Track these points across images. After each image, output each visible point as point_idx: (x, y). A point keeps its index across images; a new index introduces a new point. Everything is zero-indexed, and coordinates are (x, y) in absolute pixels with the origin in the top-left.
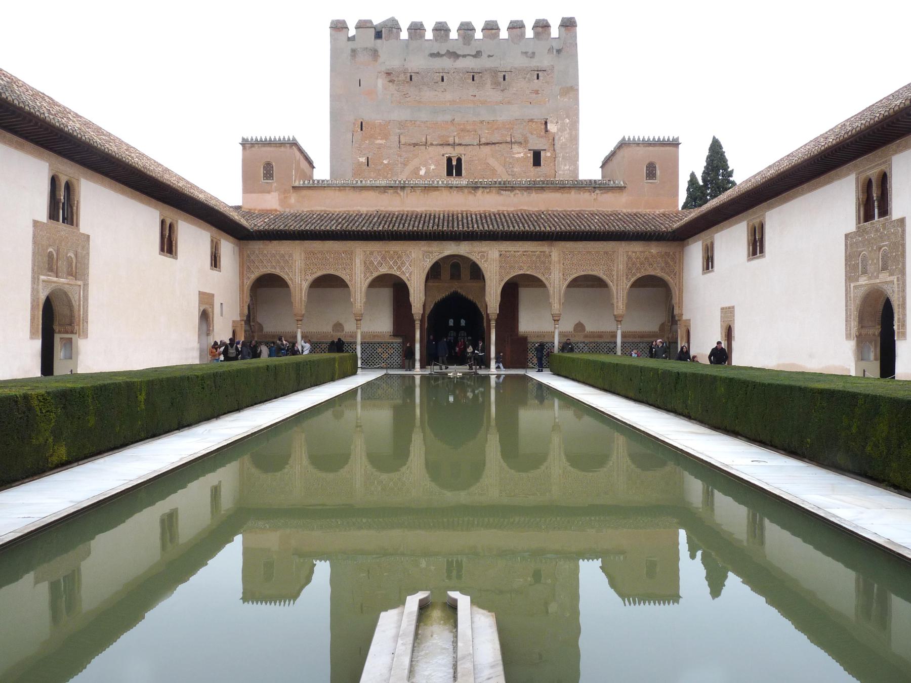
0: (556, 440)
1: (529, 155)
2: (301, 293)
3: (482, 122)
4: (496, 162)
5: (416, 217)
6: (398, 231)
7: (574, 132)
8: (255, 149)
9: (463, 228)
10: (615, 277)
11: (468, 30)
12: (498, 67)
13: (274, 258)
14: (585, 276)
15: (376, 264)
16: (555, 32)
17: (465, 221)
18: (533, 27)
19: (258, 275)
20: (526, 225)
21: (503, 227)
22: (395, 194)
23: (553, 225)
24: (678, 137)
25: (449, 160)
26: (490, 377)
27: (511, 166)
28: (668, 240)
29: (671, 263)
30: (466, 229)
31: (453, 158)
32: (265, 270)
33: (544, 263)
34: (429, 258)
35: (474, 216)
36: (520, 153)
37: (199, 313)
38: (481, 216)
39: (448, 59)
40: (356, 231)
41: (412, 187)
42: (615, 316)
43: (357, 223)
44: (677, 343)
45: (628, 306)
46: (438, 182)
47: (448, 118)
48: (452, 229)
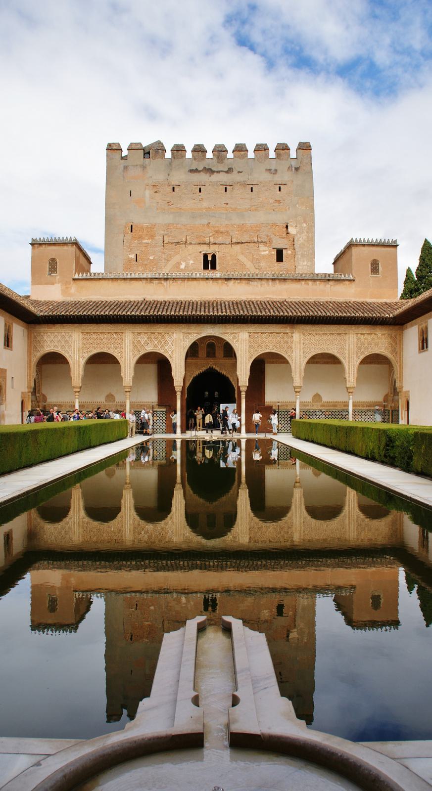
0: (298, 494)
1: (273, 253)
3: (233, 225)
4: (245, 258)
5: (177, 303)
7: (310, 234)
9: (218, 313)
10: (347, 355)
11: (222, 151)
12: (245, 181)
13: (56, 339)
14: (322, 354)
15: (143, 343)
16: (293, 154)
17: (219, 307)
18: (275, 150)
19: (43, 353)
20: (271, 311)
21: (252, 312)
23: (295, 310)
24: (396, 240)
25: (205, 256)
26: (241, 441)
27: (258, 262)
30: (220, 313)
31: (208, 255)
32: (49, 349)
34: (189, 339)
35: (227, 303)
36: (265, 251)
38: (233, 303)
39: (204, 174)
41: (174, 279)
42: (347, 389)
43: (127, 309)
44: (399, 411)
45: (358, 380)
46: (196, 274)
47: (205, 222)
48: (208, 314)
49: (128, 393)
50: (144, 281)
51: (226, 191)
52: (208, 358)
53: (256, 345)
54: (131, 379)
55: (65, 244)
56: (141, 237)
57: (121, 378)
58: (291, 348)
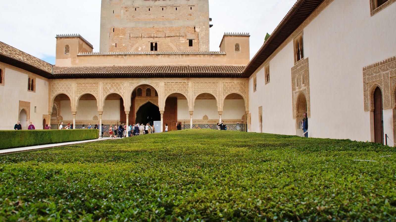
1: (187, 42)
2: (75, 102)
3: (166, 28)
6: (117, 74)
8: (62, 39)
10: (218, 94)
22: (122, 58)
25: (152, 44)
27: (179, 46)
28: (242, 77)
29: (244, 88)
33: (185, 87)
37: (19, 111)
40: (99, 74)
41: (129, 55)
42: (219, 112)
47: (152, 26)
49: (101, 115)
50: (114, 56)
51: (163, 10)
52: (146, 97)
53: (168, 89)
54: (102, 107)
55: (73, 37)
56: (118, 34)
57: (97, 107)
58: (188, 90)
